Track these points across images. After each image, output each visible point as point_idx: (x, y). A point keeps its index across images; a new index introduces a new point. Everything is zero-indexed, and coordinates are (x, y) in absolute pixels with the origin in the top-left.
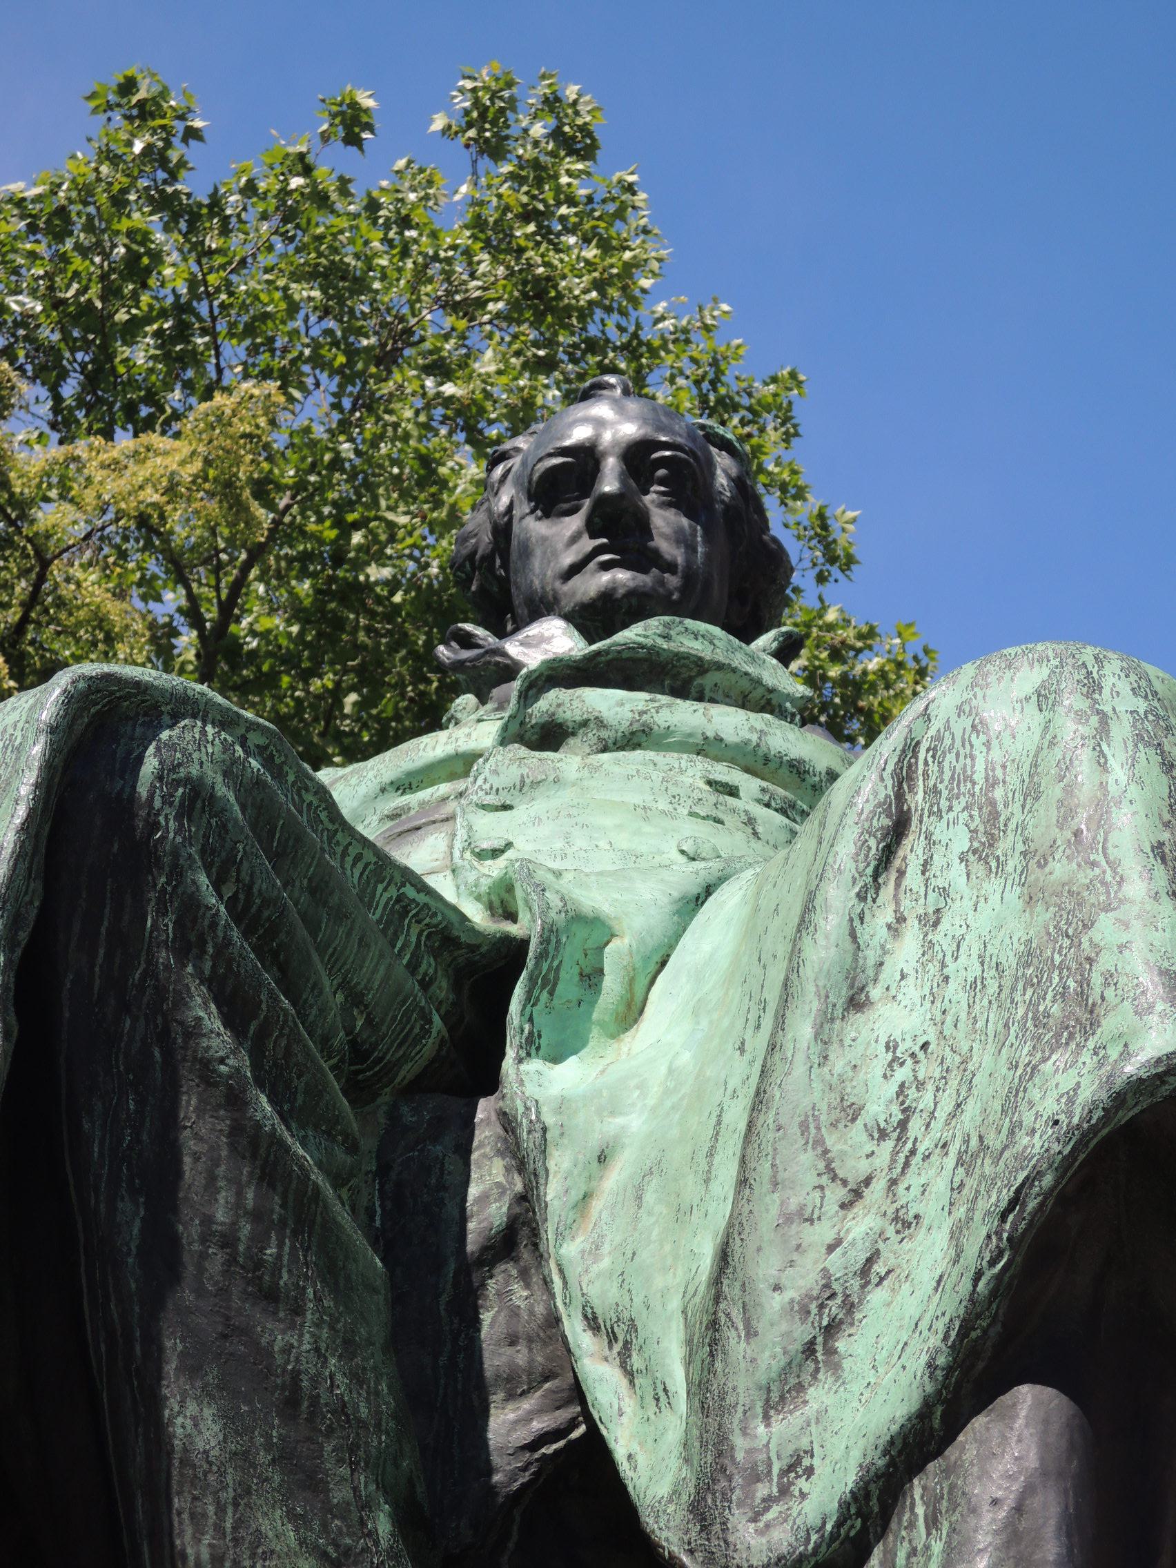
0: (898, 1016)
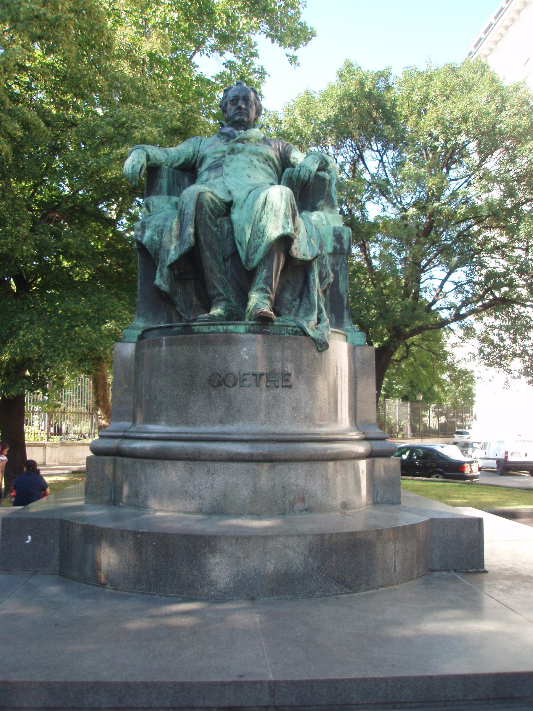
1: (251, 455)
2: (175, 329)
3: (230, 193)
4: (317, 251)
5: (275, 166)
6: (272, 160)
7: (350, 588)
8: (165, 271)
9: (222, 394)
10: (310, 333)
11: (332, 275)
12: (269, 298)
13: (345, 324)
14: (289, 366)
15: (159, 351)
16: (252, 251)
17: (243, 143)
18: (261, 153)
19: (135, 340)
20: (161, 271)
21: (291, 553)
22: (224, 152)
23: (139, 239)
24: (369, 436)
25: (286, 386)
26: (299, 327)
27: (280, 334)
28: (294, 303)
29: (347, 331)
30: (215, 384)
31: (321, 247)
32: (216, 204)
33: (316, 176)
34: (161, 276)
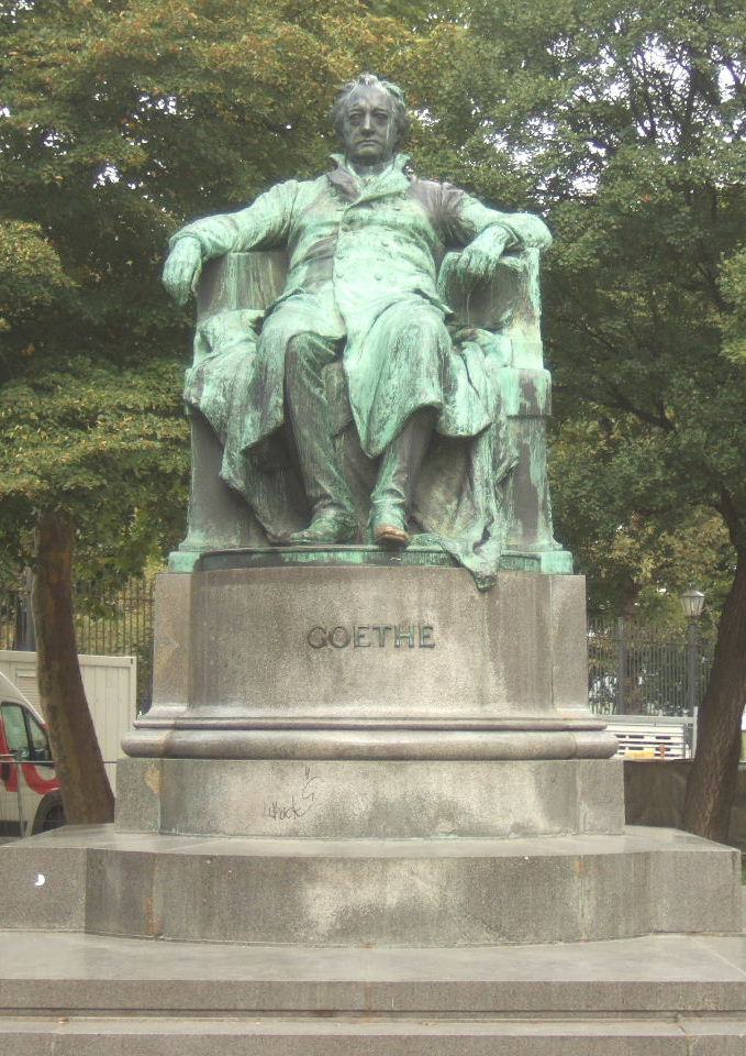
0: (394, 382)
1: (371, 748)
2: (254, 557)
3: (342, 318)
4: (485, 420)
5: (429, 241)
6: (423, 233)
7: (509, 938)
8: (236, 455)
9: (327, 659)
10: (468, 562)
11: (516, 453)
12: (401, 506)
13: (540, 537)
14: (429, 613)
15: (230, 590)
16: (375, 427)
17: (371, 207)
18: (403, 225)
19: (189, 569)
20: (229, 455)
21: (420, 884)
22: (337, 224)
23: (194, 401)
24: (571, 724)
25: (425, 646)
26: (447, 552)
27: (418, 564)
28: (448, 507)
29: (542, 548)
30: (316, 644)
31: (498, 408)
32: (319, 349)
33: (499, 266)
34: (231, 463)
